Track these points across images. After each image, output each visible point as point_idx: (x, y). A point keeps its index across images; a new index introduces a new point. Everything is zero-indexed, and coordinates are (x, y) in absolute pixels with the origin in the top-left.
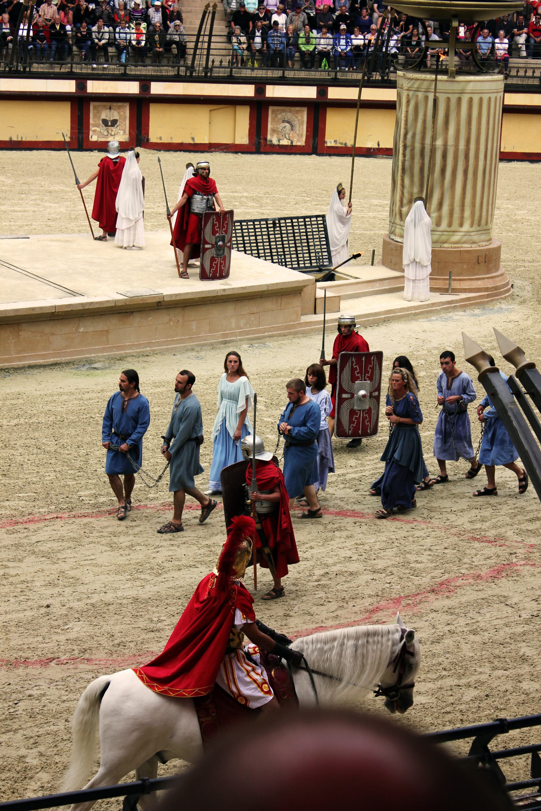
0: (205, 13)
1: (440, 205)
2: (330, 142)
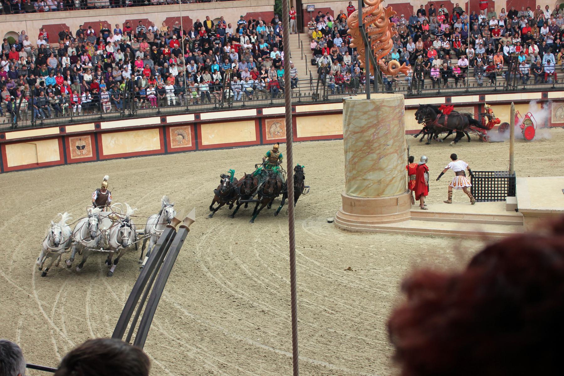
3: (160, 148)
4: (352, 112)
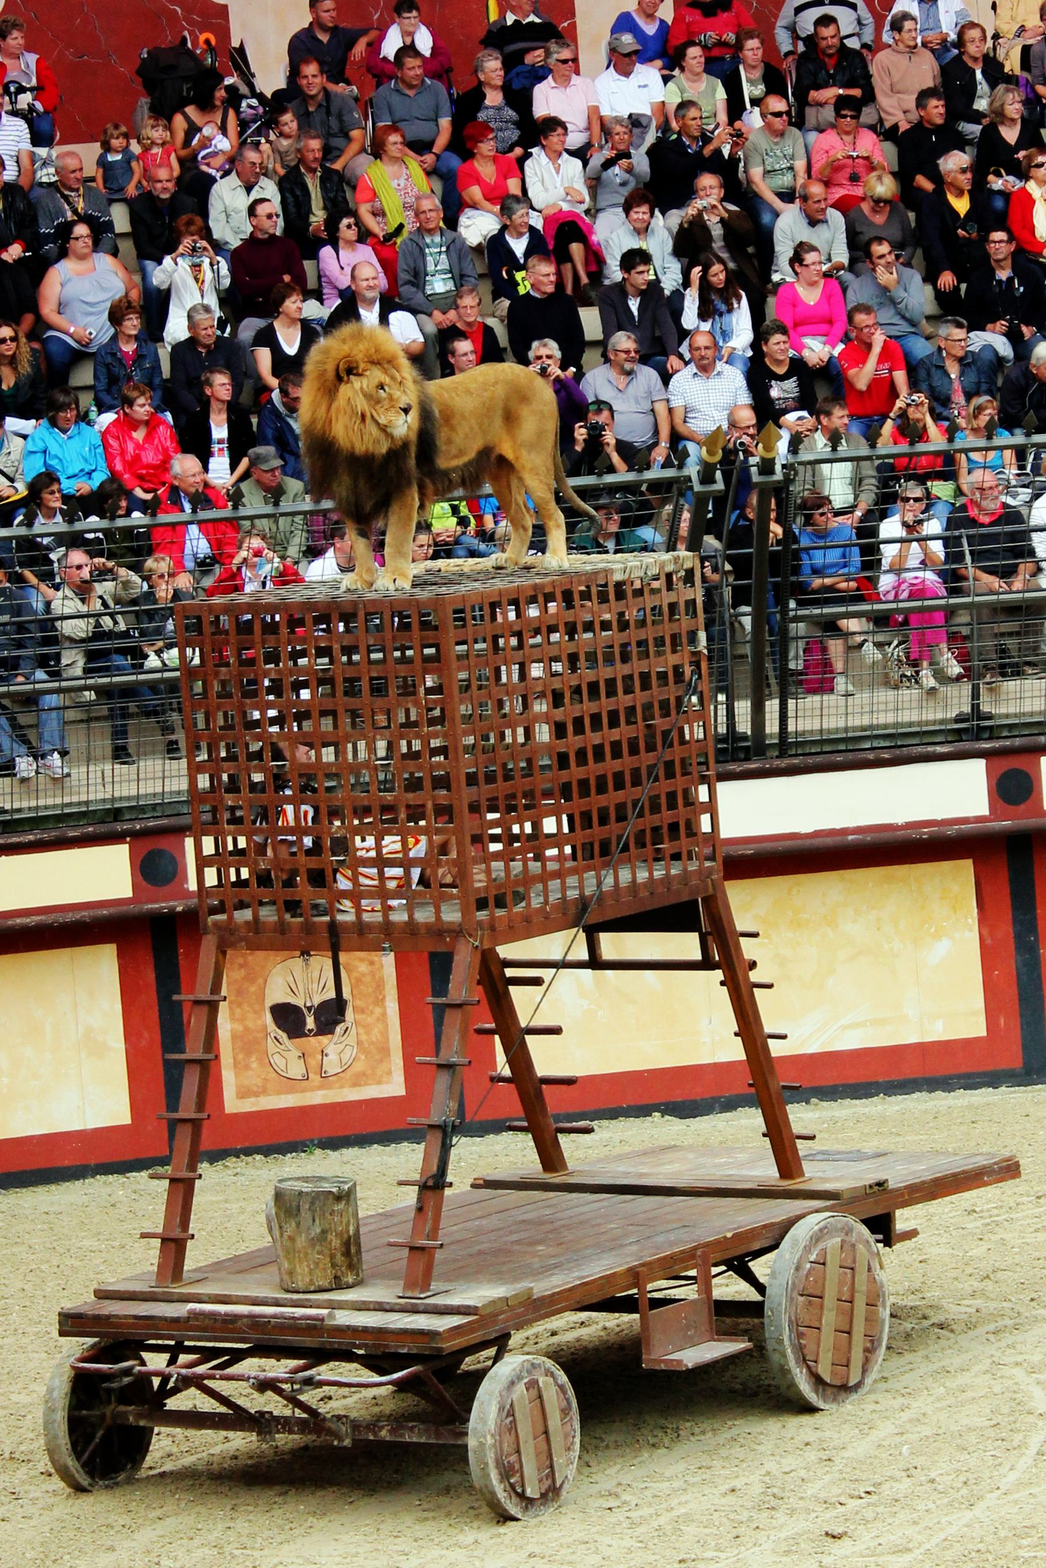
3: (978, 1028)
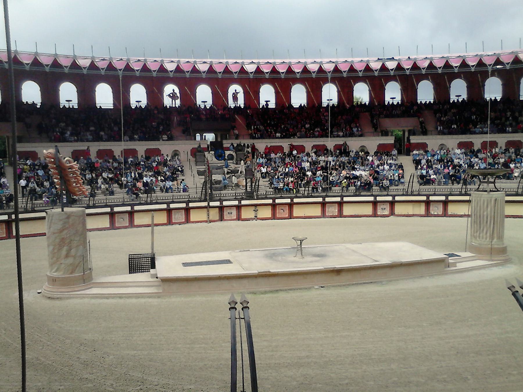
0: (411, 176)
1: (486, 233)
2: (449, 213)
4: (52, 220)
